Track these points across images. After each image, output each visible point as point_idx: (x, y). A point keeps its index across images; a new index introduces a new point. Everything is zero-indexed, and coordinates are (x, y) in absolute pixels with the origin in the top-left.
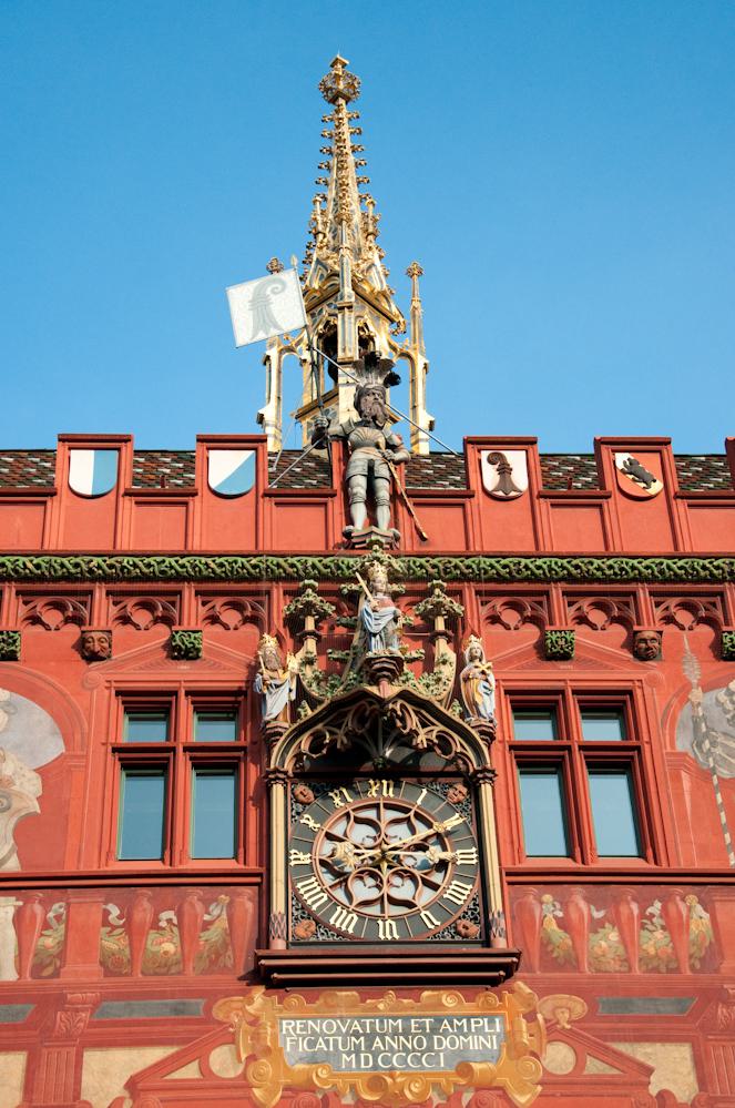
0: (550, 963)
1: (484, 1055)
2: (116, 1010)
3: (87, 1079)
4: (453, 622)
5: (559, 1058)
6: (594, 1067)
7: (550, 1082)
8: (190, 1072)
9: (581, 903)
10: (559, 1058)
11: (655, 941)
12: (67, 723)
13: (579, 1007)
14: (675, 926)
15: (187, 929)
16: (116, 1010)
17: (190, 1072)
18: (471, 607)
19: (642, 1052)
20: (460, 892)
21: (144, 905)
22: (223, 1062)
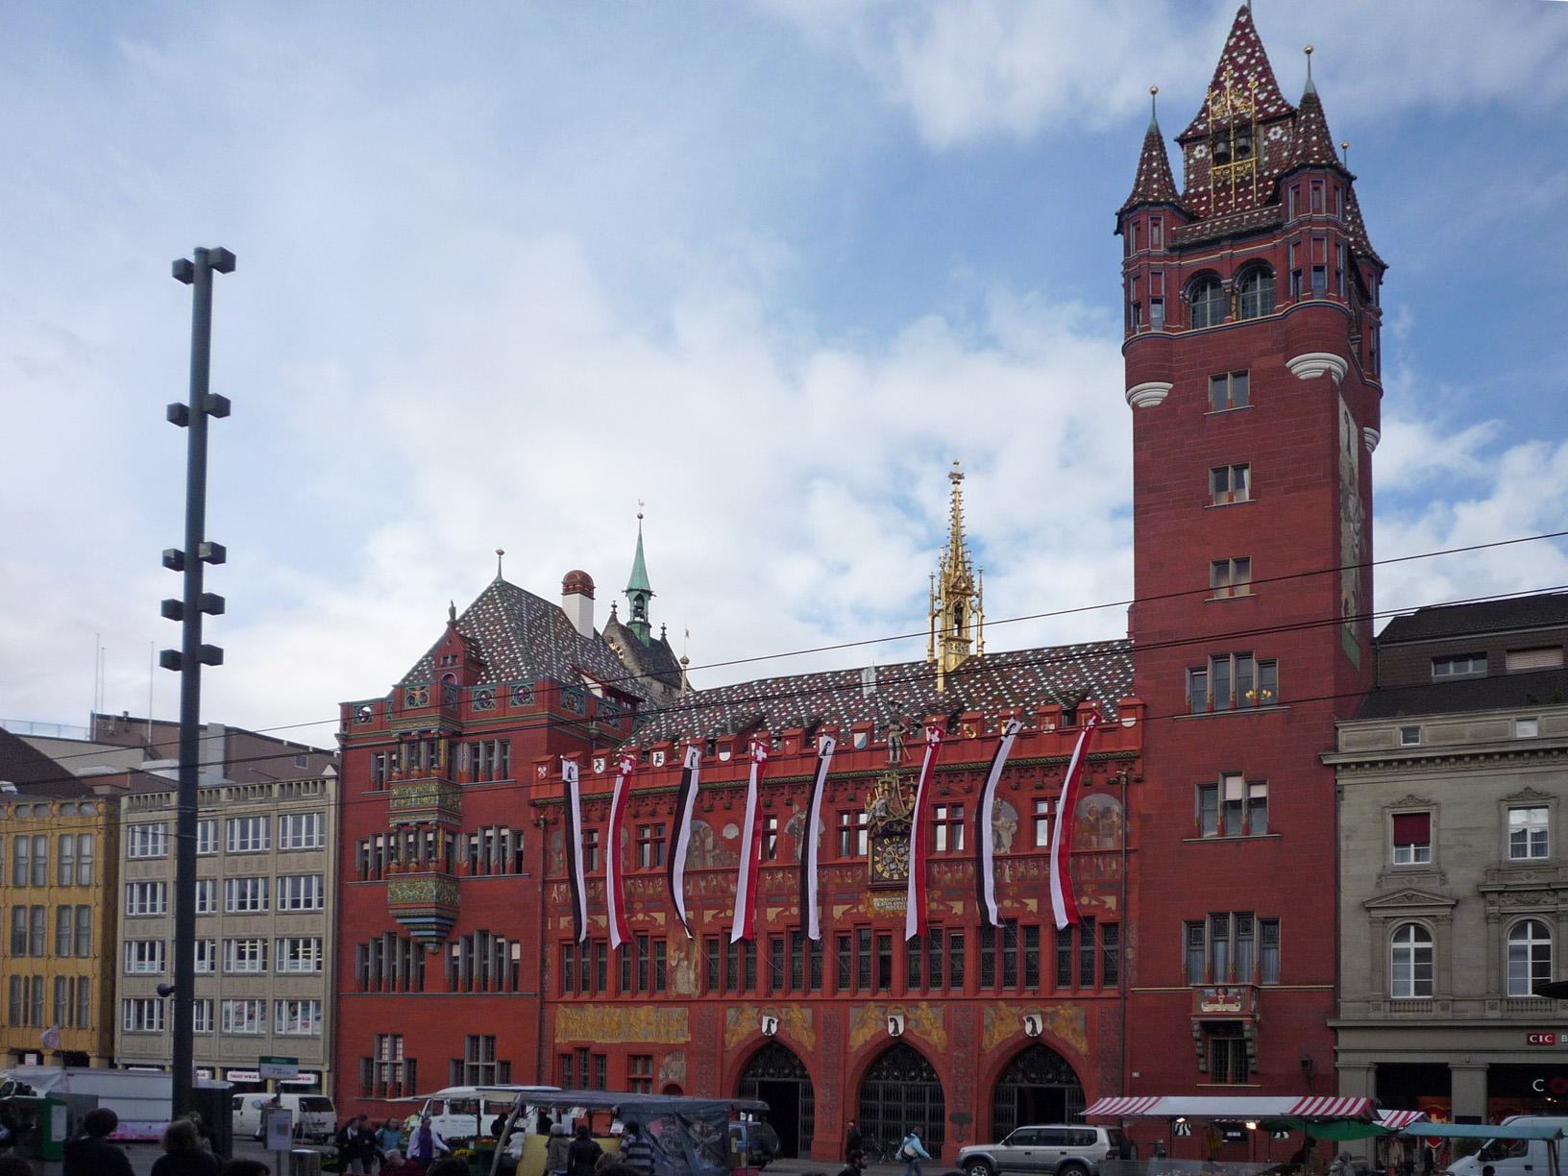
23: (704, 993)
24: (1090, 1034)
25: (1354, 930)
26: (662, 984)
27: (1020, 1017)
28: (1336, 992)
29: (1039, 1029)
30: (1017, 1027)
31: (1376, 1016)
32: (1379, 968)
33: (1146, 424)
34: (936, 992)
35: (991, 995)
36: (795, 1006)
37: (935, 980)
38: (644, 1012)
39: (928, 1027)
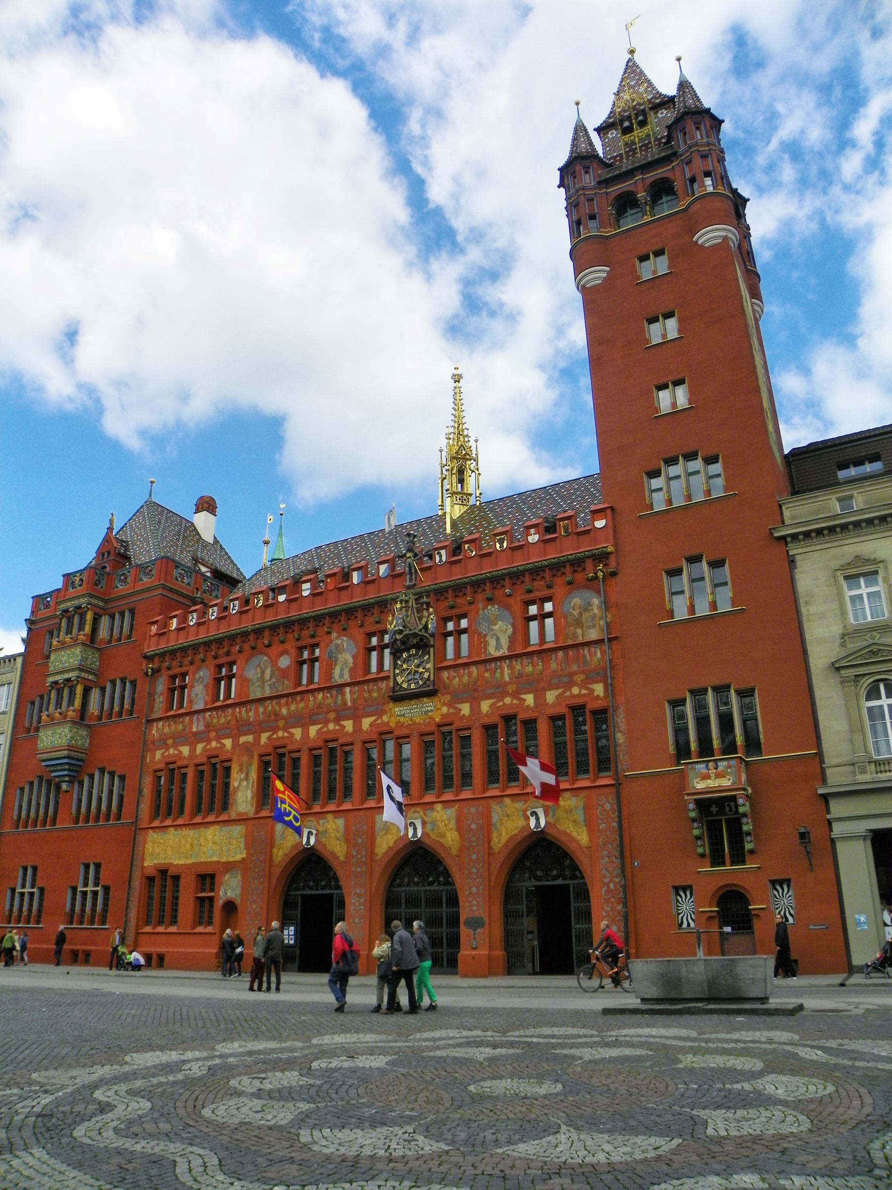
0: (445, 688)
1: (432, 711)
2: (367, 709)
3: (363, 724)
4: (428, 604)
5: (445, 710)
6: (451, 710)
7: (442, 715)
8: (379, 721)
9: (453, 673)
10: (445, 710)
11: (465, 679)
12: (356, 643)
13: (449, 697)
14: (470, 675)
15: (379, 690)
16: (367, 709)
17: (379, 721)
18: (431, 600)
19: (460, 706)
20: (426, 675)
21: (371, 685)
22: (385, 718)
23: (257, 812)
24: (590, 824)
25: (829, 696)
26: (225, 806)
27: (525, 811)
28: (820, 756)
29: (543, 823)
30: (521, 823)
31: (867, 777)
32: (856, 728)
33: (593, 300)
34: (448, 796)
35: (496, 793)
36: (330, 817)
37: (447, 782)
38: (211, 833)
39: (443, 829)
